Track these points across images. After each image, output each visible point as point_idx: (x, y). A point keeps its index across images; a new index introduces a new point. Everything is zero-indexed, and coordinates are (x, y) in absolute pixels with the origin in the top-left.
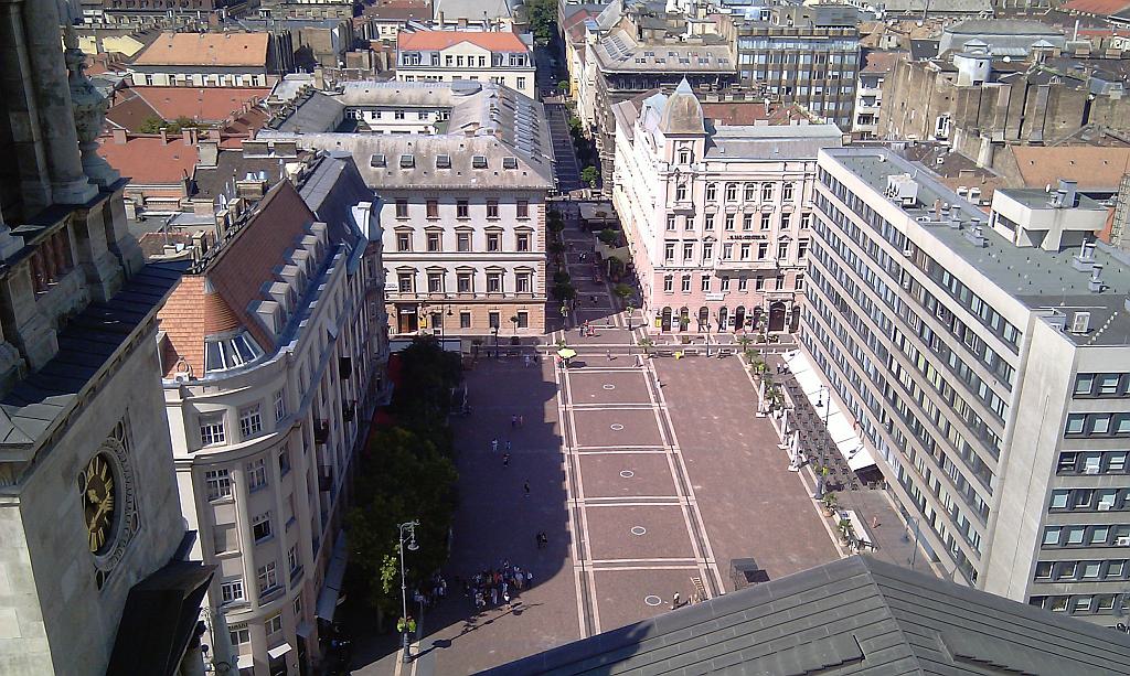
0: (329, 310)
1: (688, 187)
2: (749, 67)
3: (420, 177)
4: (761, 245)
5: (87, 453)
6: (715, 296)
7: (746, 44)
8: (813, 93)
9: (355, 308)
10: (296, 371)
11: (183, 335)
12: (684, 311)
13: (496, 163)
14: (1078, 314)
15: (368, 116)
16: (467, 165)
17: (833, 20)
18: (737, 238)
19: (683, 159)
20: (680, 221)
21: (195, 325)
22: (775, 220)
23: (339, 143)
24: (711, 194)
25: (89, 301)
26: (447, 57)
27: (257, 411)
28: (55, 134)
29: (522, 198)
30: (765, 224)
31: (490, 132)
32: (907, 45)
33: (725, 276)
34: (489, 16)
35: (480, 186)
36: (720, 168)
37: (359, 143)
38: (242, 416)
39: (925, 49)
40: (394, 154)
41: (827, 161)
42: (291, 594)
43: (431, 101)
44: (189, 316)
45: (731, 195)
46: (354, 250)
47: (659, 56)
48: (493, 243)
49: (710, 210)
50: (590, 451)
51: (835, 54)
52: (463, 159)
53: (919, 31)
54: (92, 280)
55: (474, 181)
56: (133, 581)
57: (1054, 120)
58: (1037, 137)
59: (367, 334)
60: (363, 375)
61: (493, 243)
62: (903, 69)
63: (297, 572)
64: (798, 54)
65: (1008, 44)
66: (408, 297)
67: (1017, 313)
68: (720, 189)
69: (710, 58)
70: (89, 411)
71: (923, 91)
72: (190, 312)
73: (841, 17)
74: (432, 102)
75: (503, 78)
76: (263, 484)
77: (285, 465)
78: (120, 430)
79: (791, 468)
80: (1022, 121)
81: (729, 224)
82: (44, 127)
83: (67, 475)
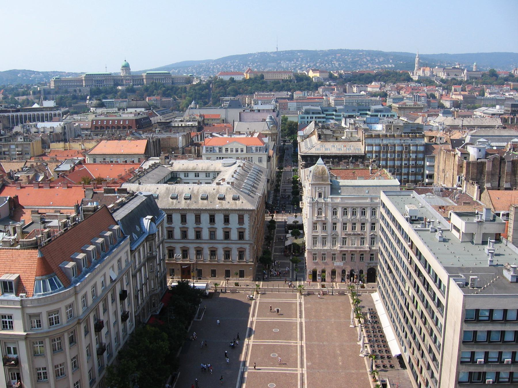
0: (113, 267)
1: (324, 209)
2: (371, 152)
3: (192, 204)
4: (362, 238)
6: (338, 264)
7: (369, 141)
8: (403, 164)
9: (137, 267)
10: (80, 296)
11: (26, 276)
12: (324, 271)
13: (229, 197)
14: (471, 277)
15: (182, 176)
16: (214, 199)
17: (411, 130)
18: (350, 234)
19: (320, 196)
20: (319, 227)
21: (32, 272)
22: (368, 226)
23: (157, 188)
24: (335, 213)
26: (226, 149)
27: (57, 314)
29: (241, 214)
30: (362, 228)
31: (228, 183)
32: (449, 142)
33: (343, 254)
34: (250, 130)
35: (220, 208)
36: (338, 201)
37: (167, 189)
38: (49, 316)
39: (456, 143)
40: (182, 193)
41: (384, 198)
43: (212, 169)
44: (30, 268)
45: (345, 213)
46: (138, 239)
47: (327, 147)
48: (227, 235)
51: (413, 145)
52: (214, 195)
53: (457, 135)
55: (218, 206)
57: (515, 177)
58: (507, 185)
59: (147, 279)
61: (227, 235)
64: (395, 145)
65: (499, 141)
67: (443, 275)
68: (339, 212)
69: (352, 148)
71: (451, 163)
72: (31, 266)
73: (415, 129)
74: (212, 169)
75: (252, 158)
79: (361, 355)
80: (500, 178)
81: (344, 228)
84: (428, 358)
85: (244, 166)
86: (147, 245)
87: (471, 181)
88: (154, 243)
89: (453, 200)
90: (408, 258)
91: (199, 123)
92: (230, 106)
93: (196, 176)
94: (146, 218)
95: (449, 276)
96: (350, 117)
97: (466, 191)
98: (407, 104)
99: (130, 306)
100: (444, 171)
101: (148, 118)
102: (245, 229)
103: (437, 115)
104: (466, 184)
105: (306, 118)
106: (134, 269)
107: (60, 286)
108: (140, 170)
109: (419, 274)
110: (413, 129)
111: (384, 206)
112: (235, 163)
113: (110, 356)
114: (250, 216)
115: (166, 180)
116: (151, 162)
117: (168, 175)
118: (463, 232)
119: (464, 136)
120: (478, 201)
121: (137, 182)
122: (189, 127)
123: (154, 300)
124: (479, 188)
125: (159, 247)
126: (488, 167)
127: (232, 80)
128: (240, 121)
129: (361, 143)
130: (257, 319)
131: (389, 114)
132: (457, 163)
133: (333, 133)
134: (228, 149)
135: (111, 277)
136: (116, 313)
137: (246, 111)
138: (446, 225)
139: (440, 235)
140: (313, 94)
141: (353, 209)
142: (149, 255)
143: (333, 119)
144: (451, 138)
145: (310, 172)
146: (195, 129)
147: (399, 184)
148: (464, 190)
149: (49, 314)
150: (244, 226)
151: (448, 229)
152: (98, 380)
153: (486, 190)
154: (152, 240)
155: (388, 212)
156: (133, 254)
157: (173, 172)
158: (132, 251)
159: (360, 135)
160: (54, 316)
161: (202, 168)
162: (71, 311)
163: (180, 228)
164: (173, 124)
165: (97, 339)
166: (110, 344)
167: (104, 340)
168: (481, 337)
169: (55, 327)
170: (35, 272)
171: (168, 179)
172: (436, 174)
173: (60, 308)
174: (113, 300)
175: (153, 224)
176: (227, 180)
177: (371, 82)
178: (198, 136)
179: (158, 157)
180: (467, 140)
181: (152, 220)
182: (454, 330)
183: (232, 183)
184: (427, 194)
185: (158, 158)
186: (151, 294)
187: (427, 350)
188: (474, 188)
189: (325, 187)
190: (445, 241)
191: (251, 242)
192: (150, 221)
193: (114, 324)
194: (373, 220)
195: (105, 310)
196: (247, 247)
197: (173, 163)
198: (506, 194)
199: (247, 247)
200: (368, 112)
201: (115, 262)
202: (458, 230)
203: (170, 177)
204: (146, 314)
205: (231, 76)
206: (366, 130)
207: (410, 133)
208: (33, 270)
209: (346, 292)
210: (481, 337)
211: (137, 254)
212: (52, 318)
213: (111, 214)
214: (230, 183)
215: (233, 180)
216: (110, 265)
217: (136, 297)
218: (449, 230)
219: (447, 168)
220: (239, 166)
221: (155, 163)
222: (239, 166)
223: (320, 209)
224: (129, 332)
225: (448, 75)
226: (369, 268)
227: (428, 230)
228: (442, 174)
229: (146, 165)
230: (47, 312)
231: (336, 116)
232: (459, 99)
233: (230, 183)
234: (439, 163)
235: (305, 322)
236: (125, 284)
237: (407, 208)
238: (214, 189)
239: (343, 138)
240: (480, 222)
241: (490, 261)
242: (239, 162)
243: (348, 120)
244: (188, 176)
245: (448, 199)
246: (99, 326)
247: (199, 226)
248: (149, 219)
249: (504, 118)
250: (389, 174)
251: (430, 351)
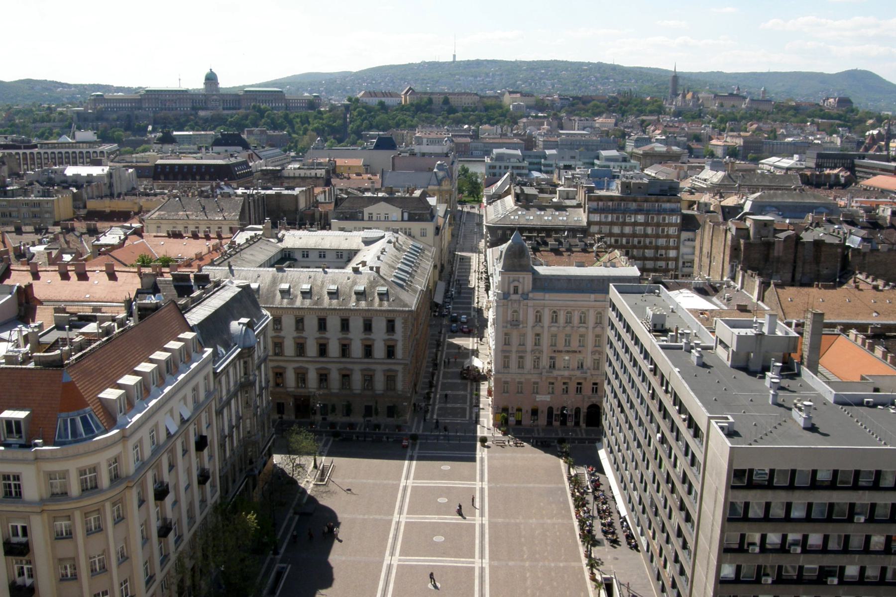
0: (184, 398)
15: (298, 256)
19: (516, 291)
24: (539, 319)
26: (370, 214)
39: (729, 213)
43: (345, 245)
45: (555, 319)
49: (538, 329)
50: (416, 518)
59: (239, 418)
60: (232, 450)
62: (707, 227)
66: (302, 391)
73: (667, 188)
75: (410, 229)
76: (99, 529)
77: (119, 519)
84: (677, 543)
85: (397, 241)
86: (240, 365)
87: (749, 272)
88: (251, 362)
89: (721, 301)
90: (649, 389)
91: (328, 172)
92: (378, 147)
93: (320, 257)
95: (710, 418)
96: (568, 167)
97: (742, 288)
98: (656, 149)
99: (212, 461)
100: (710, 255)
101: (245, 163)
102: (396, 341)
103: (702, 168)
104: (743, 277)
105: (498, 167)
106: (220, 403)
109: (666, 415)
110: (663, 188)
111: (614, 308)
112: (383, 237)
113: (179, 539)
114: (405, 322)
115: (272, 262)
116: (248, 234)
117: (277, 254)
118: (733, 351)
119: (742, 202)
120: (759, 302)
121: (226, 262)
122: (311, 178)
123: (251, 451)
124: (762, 283)
125: (259, 367)
126: (778, 251)
127: (382, 104)
128: (393, 169)
129: (582, 210)
130: (413, 483)
131: (628, 164)
132: (729, 243)
133: (539, 192)
134: (371, 214)
136: (189, 471)
137: (402, 154)
138: (709, 340)
139: (697, 355)
140: (509, 129)
141: (567, 313)
142: (243, 380)
143: (540, 171)
144: (722, 204)
145: (502, 252)
146: (321, 182)
147: (638, 274)
148: (739, 286)
149: (82, 472)
150: (395, 337)
151: (711, 345)
152: (159, 577)
153: (772, 286)
154: (249, 356)
155: (620, 317)
156: (218, 378)
157: (284, 249)
158: (215, 373)
159: (581, 196)
161: (331, 244)
162: (116, 468)
163: (294, 338)
164: (285, 173)
165: (158, 512)
166: (179, 521)
167: (170, 515)
168: (756, 511)
171: (276, 260)
172: (696, 260)
173: (99, 464)
174: (185, 452)
175: (250, 330)
176: (369, 264)
177: (599, 114)
178: (325, 192)
179: (260, 224)
180: (747, 208)
181: (249, 325)
182: (715, 501)
183: (376, 267)
184: (681, 291)
185: (260, 227)
187: (674, 532)
188: (754, 282)
189: (524, 278)
190: (704, 365)
191: (406, 362)
192: (244, 328)
193: (187, 489)
194: (596, 329)
195: (172, 467)
196: (399, 368)
197: (284, 235)
198: (803, 292)
199: (399, 368)
200: (596, 162)
201: (188, 391)
202: (726, 347)
203: (279, 257)
204: (237, 474)
205: (380, 99)
206: (590, 190)
207: (660, 195)
209: (554, 442)
210: (756, 511)
211: (223, 379)
212: (86, 479)
213: (183, 315)
214: (375, 269)
215: (378, 264)
216: (180, 395)
217: (222, 446)
218: (711, 348)
219: (714, 251)
220: (389, 242)
221: (255, 234)
222: (389, 242)
223: (515, 311)
224: (210, 501)
225: (722, 105)
226: (590, 404)
227: (680, 348)
228: (706, 261)
229: (241, 238)
230: (77, 468)
231: (546, 165)
232: (737, 144)
233: (375, 269)
234: (702, 243)
235: (490, 489)
236: (204, 426)
237: (650, 312)
238: (348, 279)
239: (555, 200)
240: (760, 334)
241: (773, 395)
242: (389, 235)
243: (563, 172)
244: (307, 256)
245: (714, 299)
246: (161, 493)
247: (324, 335)
248: (244, 324)
249: (806, 175)
250: (624, 258)
251: (679, 534)
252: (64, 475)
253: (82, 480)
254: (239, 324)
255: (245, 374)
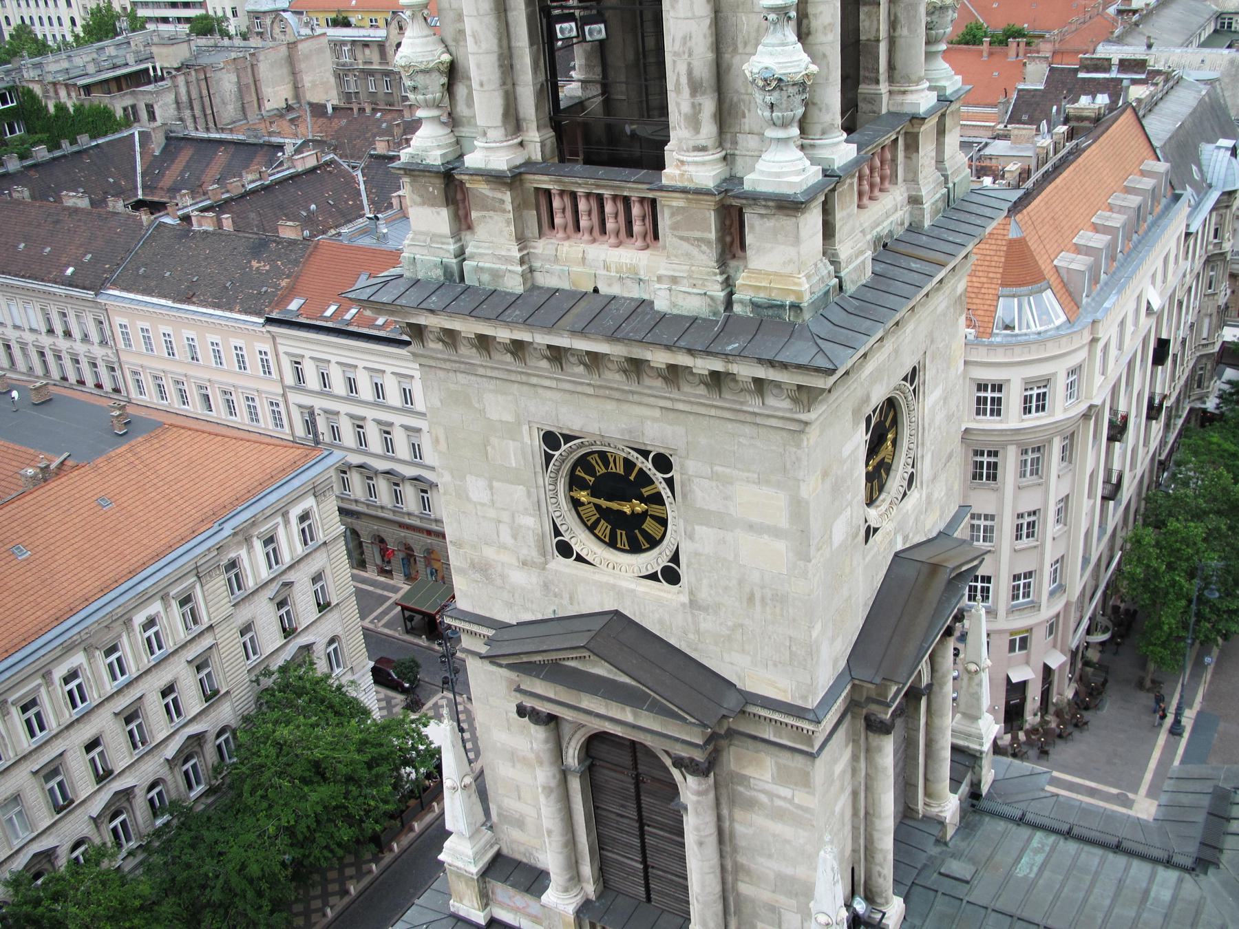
0: (1154, 276)
5: (878, 396)
11: (976, 285)
21: (991, 275)
25: (906, 224)
27: (1045, 386)
28: (903, 31)
42: (1047, 612)
44: (986, 263)
54: (915, 201)
56: (899, 547)
63: (1060, 589)
70: (889, 345)
72: (988, 258)
78: (912, 376)
82: (893, 24)
83: (856, 412)
94: (1218, 144)
99: (1167, 382)
107: (1058, 317)
108: (1123, 8)
135: (1148, 303)
142: (1210, 247)
158: (1188, 235)
160: (1035, 392)
169: (1035, 419)
170: (999, 276)
173: (1055, 374)
175: (1233, 159)
186: (1198, 354)
203: (1210, 29)
208: (993, 269)
212: (1031, 396)
248: (1227, 149)
252: (998, 387)
253: (1026, 397)
254: (1219, 148)
255: (1215, 237)
